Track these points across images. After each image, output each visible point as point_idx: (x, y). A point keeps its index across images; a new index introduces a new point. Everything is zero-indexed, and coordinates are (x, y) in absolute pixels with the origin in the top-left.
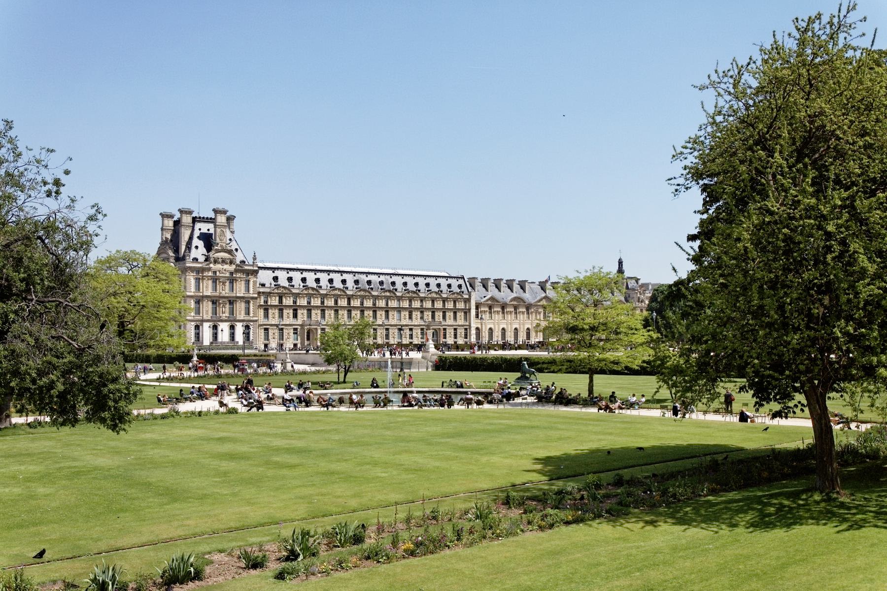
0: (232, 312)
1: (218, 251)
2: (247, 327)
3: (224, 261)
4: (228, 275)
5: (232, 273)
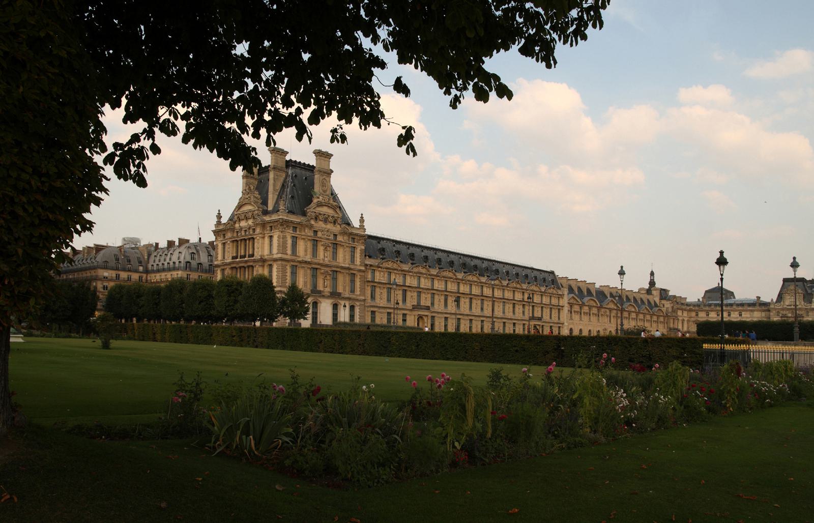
0: (335, 286)
1: (320, 205)
2: (352, 308)
3: (326, 221)
4: (332, 237)
5: (335, 235)
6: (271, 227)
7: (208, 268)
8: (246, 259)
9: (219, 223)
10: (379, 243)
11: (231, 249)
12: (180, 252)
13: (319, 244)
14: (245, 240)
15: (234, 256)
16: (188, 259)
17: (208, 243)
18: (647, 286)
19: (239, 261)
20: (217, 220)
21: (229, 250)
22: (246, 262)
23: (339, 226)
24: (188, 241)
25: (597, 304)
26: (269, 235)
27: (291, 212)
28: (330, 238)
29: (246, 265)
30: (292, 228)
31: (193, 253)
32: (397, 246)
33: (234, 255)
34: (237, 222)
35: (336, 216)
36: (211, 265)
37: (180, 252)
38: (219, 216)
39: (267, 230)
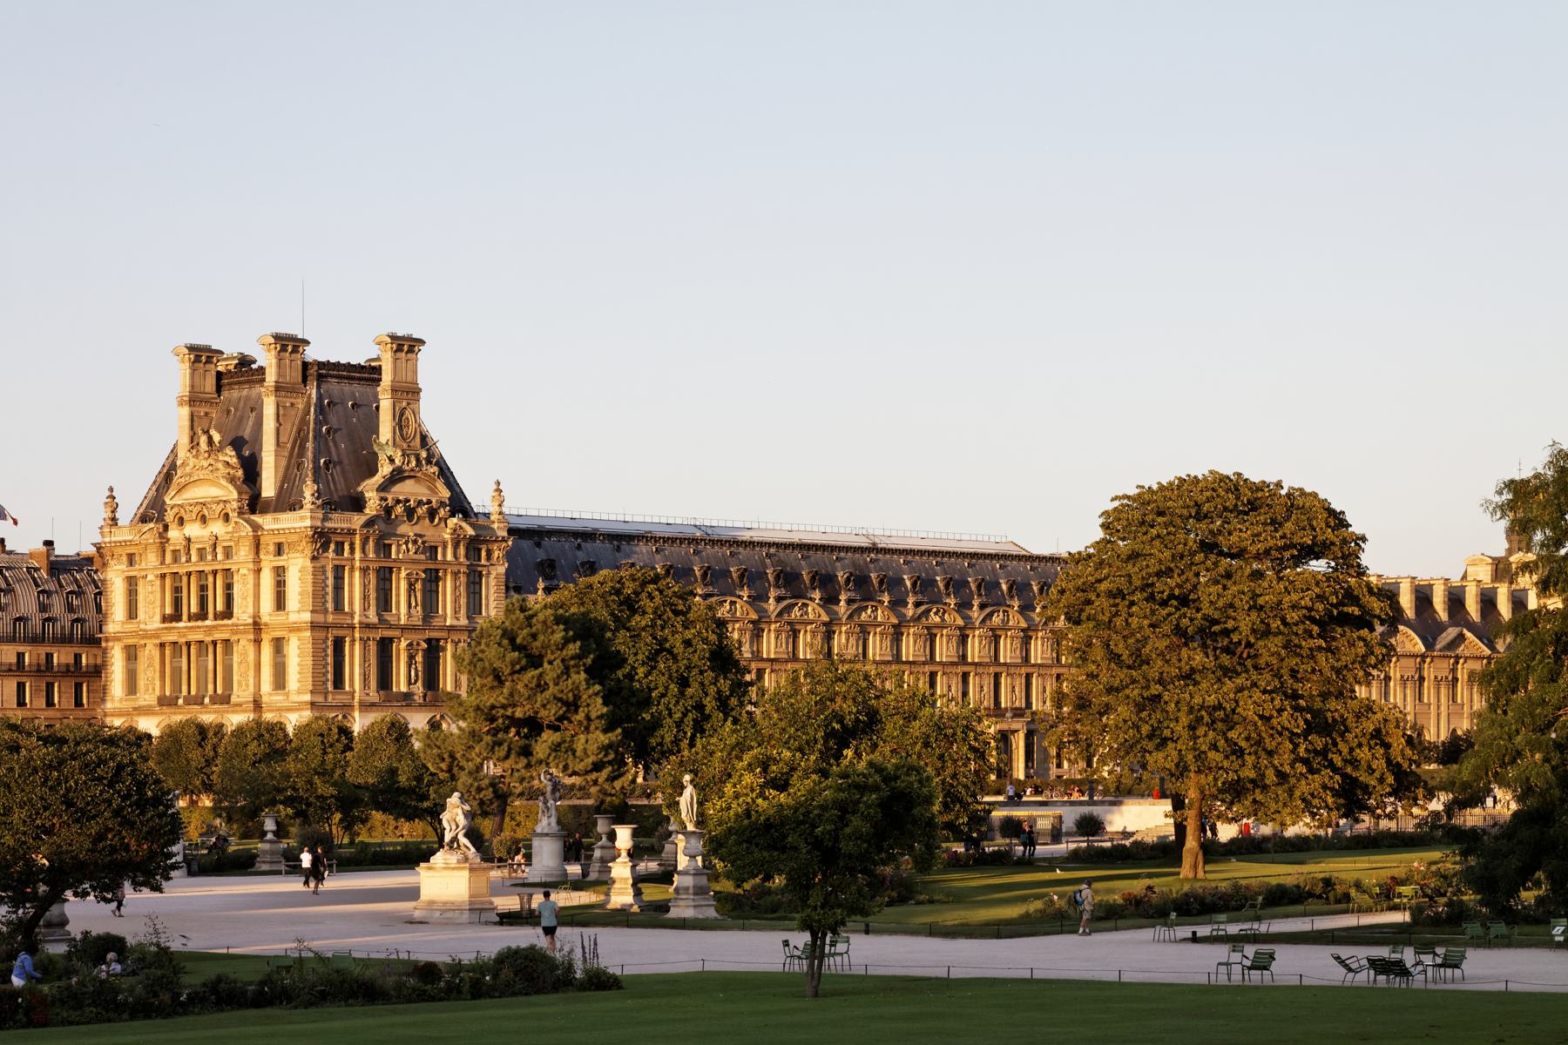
7: (39, 630)
8: (208, 623)
10: (538, 545)
22: (211, 629)
32: (588, 546)
36: (48, 619)
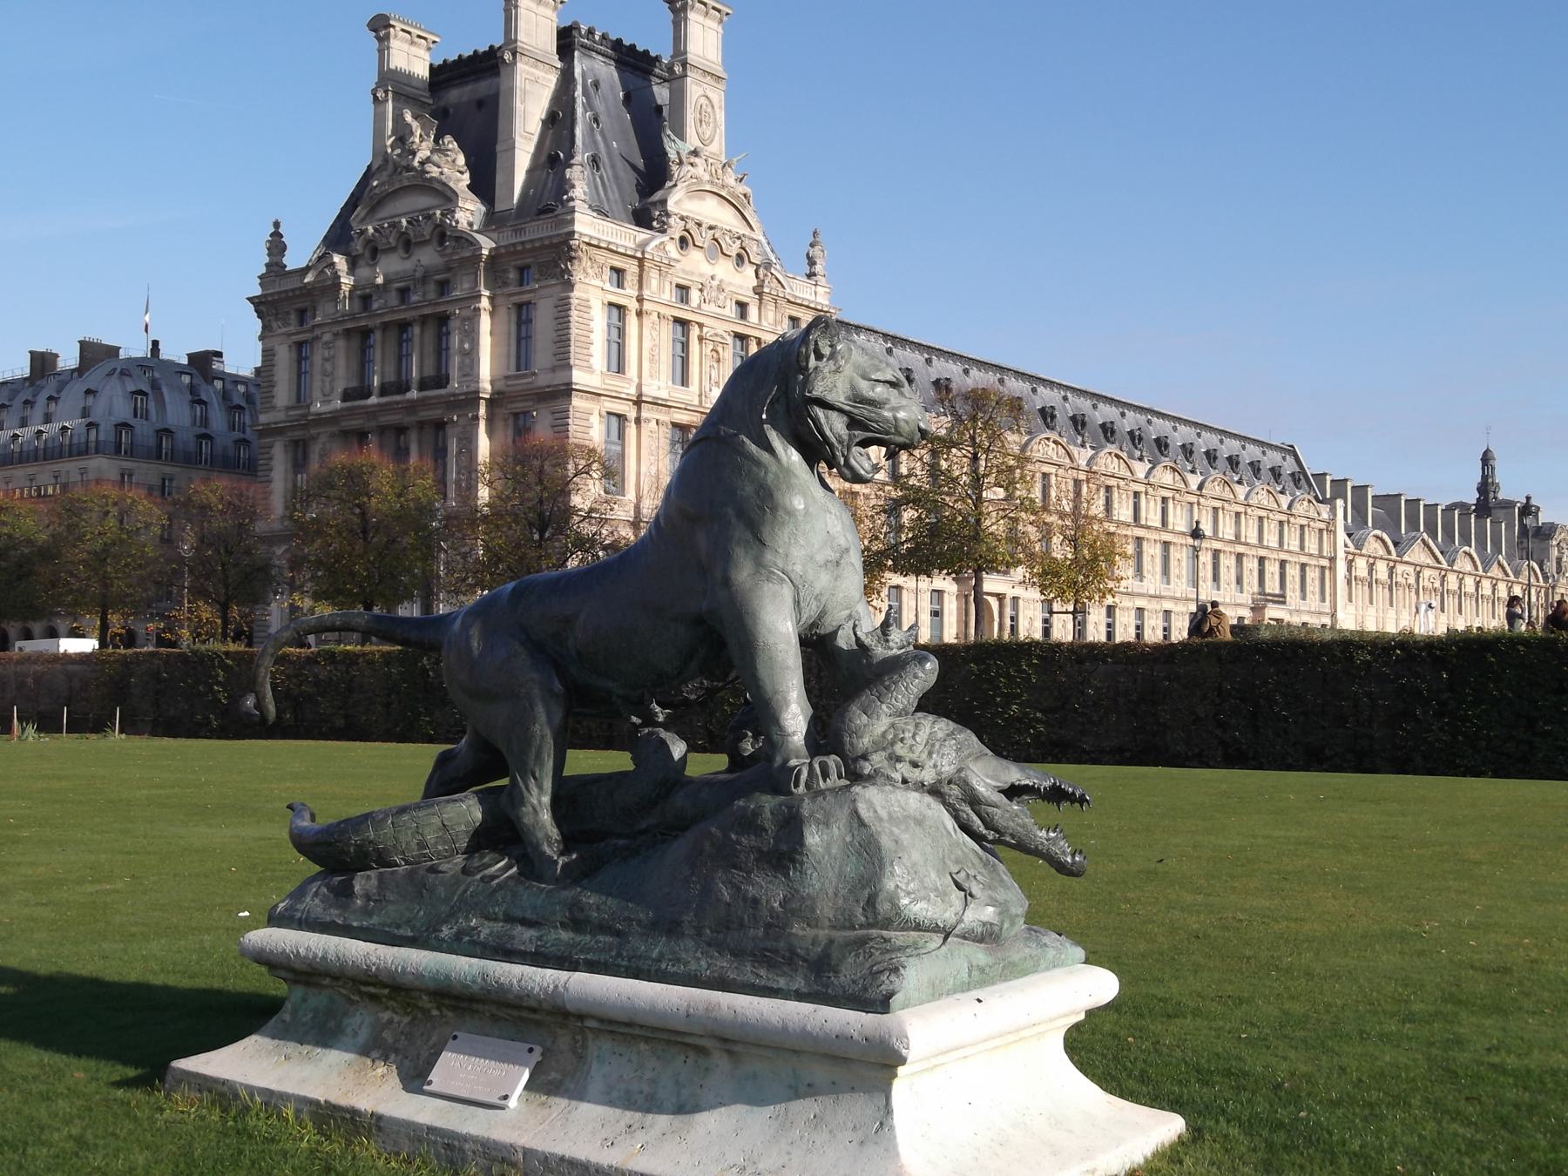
4: (731, 311)
5: (742, 307)
6: (522, 270)
7: (192, 447)
9: (275, 269)
11: (341, 363)
12: (88, 392)
13: (695, 332)
14: (404, 326)
15: (354, 389)
16: (123, 411)
17: (185, 361)
18: (1472, 497)
19: (379, 405)
20: (267, 260)
21: (328, 366)
22: (412, 406)
23: (749, 271)
24: (114, 351)
25: (1389, 553)
26: (516, 299)
27: (601, 212)
28: (727, 312)
29: (408, 420)
30: (607, 271)
31: (141, 392)
33: (354, 384)
34: (361, 262)
35: (742, 229)
37: (88, 392)
38: (277, 245)
39: (505, 284)
